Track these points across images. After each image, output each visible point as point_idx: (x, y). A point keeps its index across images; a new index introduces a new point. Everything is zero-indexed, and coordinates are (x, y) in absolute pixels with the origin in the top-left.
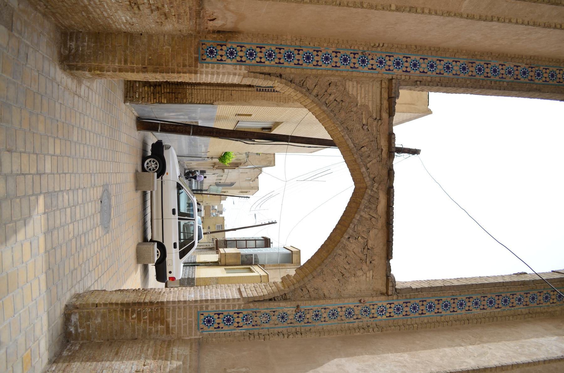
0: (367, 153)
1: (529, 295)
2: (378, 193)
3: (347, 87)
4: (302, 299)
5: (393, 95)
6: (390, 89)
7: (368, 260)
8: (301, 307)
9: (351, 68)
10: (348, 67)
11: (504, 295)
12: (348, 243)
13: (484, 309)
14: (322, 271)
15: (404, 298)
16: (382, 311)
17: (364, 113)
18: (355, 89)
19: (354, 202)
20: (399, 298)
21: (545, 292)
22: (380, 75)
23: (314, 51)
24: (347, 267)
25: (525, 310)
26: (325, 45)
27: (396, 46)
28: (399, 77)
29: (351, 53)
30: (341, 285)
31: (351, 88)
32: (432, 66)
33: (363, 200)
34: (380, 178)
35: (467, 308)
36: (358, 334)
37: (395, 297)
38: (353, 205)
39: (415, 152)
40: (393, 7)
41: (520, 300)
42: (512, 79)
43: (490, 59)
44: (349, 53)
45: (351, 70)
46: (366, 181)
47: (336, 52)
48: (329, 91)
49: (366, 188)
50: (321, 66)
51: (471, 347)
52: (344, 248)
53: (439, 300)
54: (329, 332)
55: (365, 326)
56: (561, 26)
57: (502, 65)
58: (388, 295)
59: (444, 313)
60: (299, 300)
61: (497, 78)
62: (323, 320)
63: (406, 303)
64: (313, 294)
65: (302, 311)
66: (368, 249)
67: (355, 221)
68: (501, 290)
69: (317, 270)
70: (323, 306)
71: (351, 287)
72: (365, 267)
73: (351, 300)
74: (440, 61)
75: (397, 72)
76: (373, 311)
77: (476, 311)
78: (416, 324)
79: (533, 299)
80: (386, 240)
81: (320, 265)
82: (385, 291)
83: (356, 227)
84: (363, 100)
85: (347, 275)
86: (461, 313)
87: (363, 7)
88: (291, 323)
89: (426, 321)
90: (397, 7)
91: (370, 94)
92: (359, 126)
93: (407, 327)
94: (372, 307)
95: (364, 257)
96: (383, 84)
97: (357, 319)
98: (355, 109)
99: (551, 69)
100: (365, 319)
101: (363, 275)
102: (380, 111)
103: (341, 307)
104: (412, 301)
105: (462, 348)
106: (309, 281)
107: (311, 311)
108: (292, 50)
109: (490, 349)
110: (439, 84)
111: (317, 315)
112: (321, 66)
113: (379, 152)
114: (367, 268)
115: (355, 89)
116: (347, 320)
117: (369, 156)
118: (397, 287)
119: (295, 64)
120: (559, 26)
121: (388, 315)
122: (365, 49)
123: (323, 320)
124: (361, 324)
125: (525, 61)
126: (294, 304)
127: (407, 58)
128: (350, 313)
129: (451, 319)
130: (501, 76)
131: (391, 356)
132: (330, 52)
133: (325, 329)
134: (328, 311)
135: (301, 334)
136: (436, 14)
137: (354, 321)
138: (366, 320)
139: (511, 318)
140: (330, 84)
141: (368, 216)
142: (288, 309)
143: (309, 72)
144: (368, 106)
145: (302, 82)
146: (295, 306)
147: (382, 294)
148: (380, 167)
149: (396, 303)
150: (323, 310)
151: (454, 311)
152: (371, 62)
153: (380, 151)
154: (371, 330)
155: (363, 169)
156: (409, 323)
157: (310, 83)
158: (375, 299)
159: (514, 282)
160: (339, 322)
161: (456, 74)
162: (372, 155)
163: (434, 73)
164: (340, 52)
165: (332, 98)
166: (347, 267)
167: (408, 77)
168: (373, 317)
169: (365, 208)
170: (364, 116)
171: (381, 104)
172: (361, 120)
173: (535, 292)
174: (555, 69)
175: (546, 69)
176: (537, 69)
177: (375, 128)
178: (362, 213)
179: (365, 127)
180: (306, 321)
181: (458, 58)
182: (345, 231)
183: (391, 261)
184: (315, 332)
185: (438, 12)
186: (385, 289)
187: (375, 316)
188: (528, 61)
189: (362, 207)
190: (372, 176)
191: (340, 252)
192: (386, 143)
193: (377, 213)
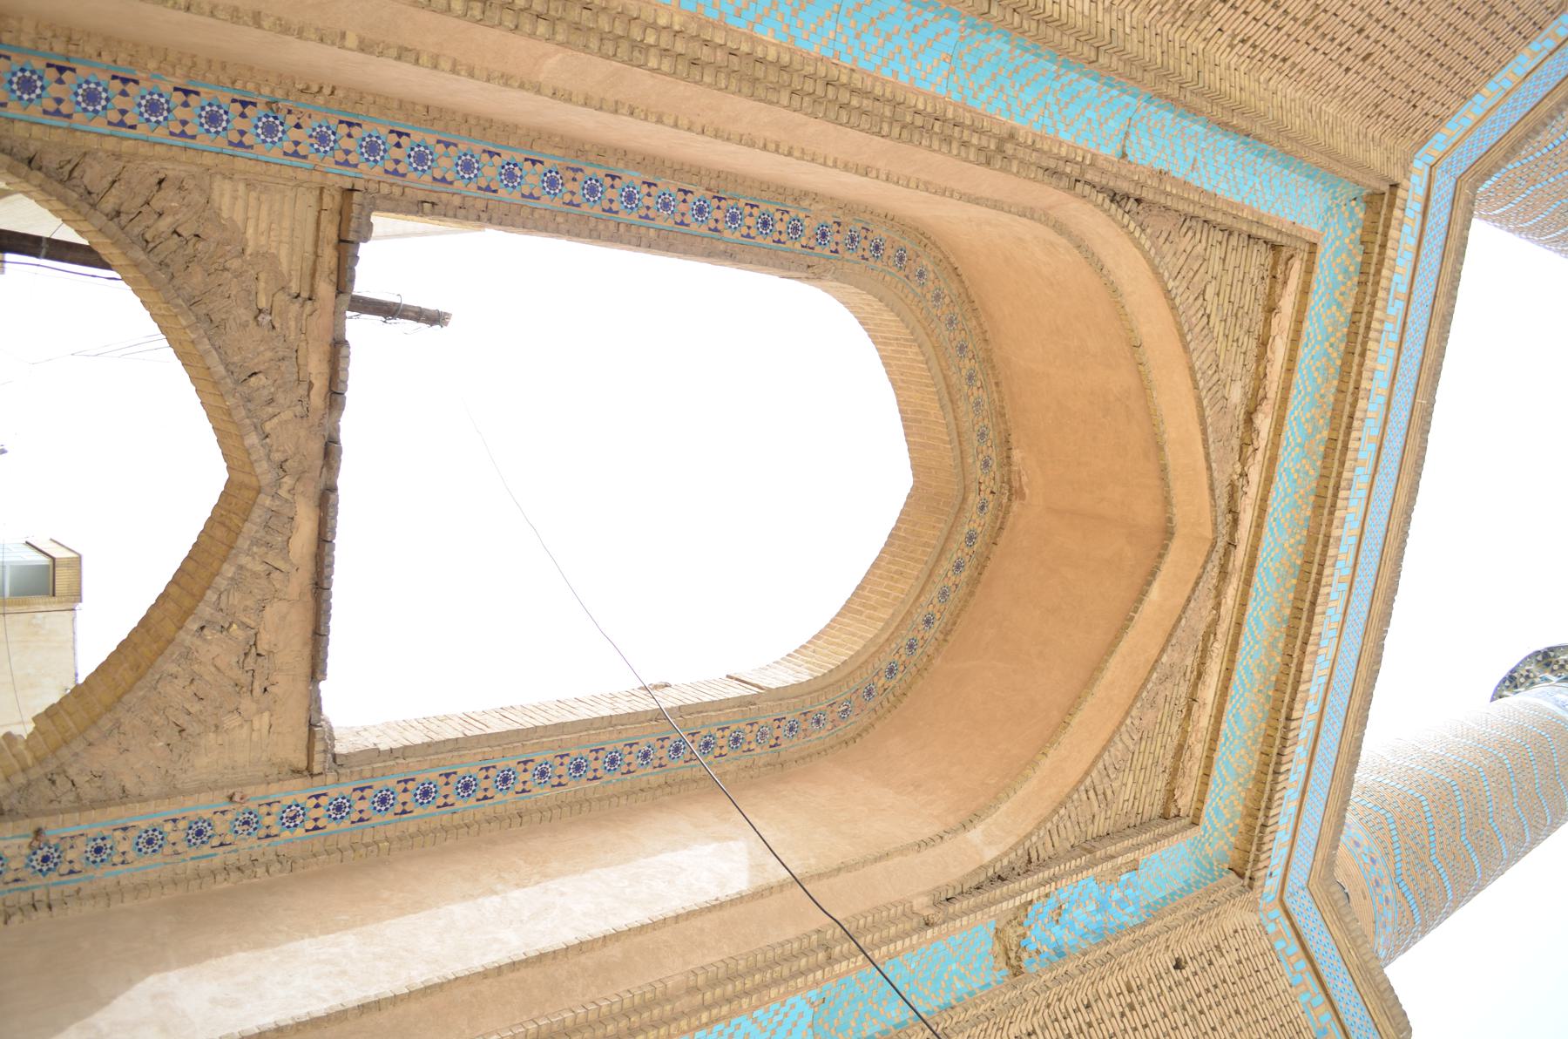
0: (266, 392)
1: (667, 743)
2: (293, 504)
3: (215, 195)
4: (51, 806)
5: (351, 237)
6: (343, 216)
7: (256, 684)
8: (48, 833)
9: (231, 143)
10: (221, 142)
11: (609, 748)
12: (198, 642)
13: (560, 785)
14: (118, 725)
15: (356, 777)
16: (293, 818)
17: (262, 276)
18: (240, 204)
19: (223, 524)
20: (343, 779)
21: (704, 733)
22: (317, 177)
23: (114, 77)
24: (195, 708)
25: (656, 778)
26: (152, 65)
27: (370, 98)
28: (372, 186)
29: (234, 101)
30: (175, 758)
31: (229, 199)
32: (467, 167)
33: (247, 525)
34: (300, 462)
35: (519, 787)
36: (225, 885)
37: (331, 777)
38: (220, 533)
39: (435, 319)
40: (352, 40)
41: (646, 755)
42: (669, 224)
43: (621, 165)
45: (229, 150)
46: (258, 471)
47: (187, 92)
48: (157, 204)
49: (259, 491)
50: (133, 127)
51: (517, 893)
52: (187, 655)
53: (447, 775)
54: (137, 890)
55: (245, 861)
56: (778, 146)
57: (650, 185)
58: (312, 775)
59: (460, 805)
60: (44, 814)
61: (634, 217)
62: (117, 859)
63: (362, 789)
64: (89, 791)
65: (53, 842)
67: (221, 582)
68: (603, 737)
69: (101, 723)
70: (120, 823)
71: (206, 760)
72: (246, 704)
73: (203, 797)
74: (491, 154)
75: (369, 172)
76: (267, 821)
77: (542, 793)
78: (387, 839)
79: (677, 750)
80: (310, 629)
81: (109, 709)
82: (303, 765)
83: (224, 597)
84: (263, 240)
85: (194, 728)
86: (505, 800)
87: (259, 26)
88: (16, 880)
89: (412, 829)
90: (361, 41)
91: (286, 223)
92: (245, 315)
93: (363, 851)
94: (265, 809)
95: (245, 679)
96: (326, 199)
97: (222, 845)
98: (235, 264)
99: (763, 207)
100: (244, 845)
101: (241, 726)
102: (313, 276)
103: (174, 821)
104: (378, 784)
105: (496, 899)
106: (76, 754)
107: (79, 842)
108: (39, 64)
109: (562, 894)
110: (483, 215)
111: (98, 850)
112: (133, 127)
113: (302, 390)
114: (254, 707)
115: (240, 204)
116: (193, 852)
117: (272, 400)
118: (340, 748)
119: (45, 112)
120: (772, 146)
121: (310, 825)
122: (279, 94)
123: (117, 859)
124: (232, 858)
125: (705, 180)
126: (28, 826)
127: (400, 134)
128: (199, 833)
129: (478, 817)
130: (643, 212)
131: (308, 946)
132: (166, 88)
133: (123, 882)
134: (132, 834)
135: (50, 907)
136: (471, 75)
138: (248, 845)
139: (623, 801)
140: (161, 182)
141: (260, 568)
142: (7, 843)
143: (92, 142)
144: (275, 257)
145: (69, 167)
146: (30, 832)
147: (296, 772)
148: (303, 433)
149: (334, 792)
150: (119, 834)
151: (485, 798)
152: (295, 134)
153: (305, 386)
154: (260, 871)
155: (252, 439)
156: (367, 839)
157: (93, 175)
158: (275, 787)
159: (636, 714)
160: (168, 860)
161: (531, 196)
162: (281, 398)
163: (473, 186)
164: (197, 93)
165: (165, 224)
166: (195, 708)
167: (397, 191)
168: (268, 836)
169: (252, 544)
170: (262, 285)
171: (317, 256)
172: (251, 295)
174: (772, 210)
175: (752, 206)
176: (731, 202)
177: (292, 324)
178: (244, 560)
179: (265, 319)
180: (64, 868)
181: (541, 153)
182: (189, 612)
183: (322, 685)
184: (94, 897)
185: (477, 72)
186: (304, 758)
187: (274, 831)
188: (713, 183)
189: (243, 543)
190: (277, 457)
191: (173, 668)
192: (325, 368)
193: (286, 559)
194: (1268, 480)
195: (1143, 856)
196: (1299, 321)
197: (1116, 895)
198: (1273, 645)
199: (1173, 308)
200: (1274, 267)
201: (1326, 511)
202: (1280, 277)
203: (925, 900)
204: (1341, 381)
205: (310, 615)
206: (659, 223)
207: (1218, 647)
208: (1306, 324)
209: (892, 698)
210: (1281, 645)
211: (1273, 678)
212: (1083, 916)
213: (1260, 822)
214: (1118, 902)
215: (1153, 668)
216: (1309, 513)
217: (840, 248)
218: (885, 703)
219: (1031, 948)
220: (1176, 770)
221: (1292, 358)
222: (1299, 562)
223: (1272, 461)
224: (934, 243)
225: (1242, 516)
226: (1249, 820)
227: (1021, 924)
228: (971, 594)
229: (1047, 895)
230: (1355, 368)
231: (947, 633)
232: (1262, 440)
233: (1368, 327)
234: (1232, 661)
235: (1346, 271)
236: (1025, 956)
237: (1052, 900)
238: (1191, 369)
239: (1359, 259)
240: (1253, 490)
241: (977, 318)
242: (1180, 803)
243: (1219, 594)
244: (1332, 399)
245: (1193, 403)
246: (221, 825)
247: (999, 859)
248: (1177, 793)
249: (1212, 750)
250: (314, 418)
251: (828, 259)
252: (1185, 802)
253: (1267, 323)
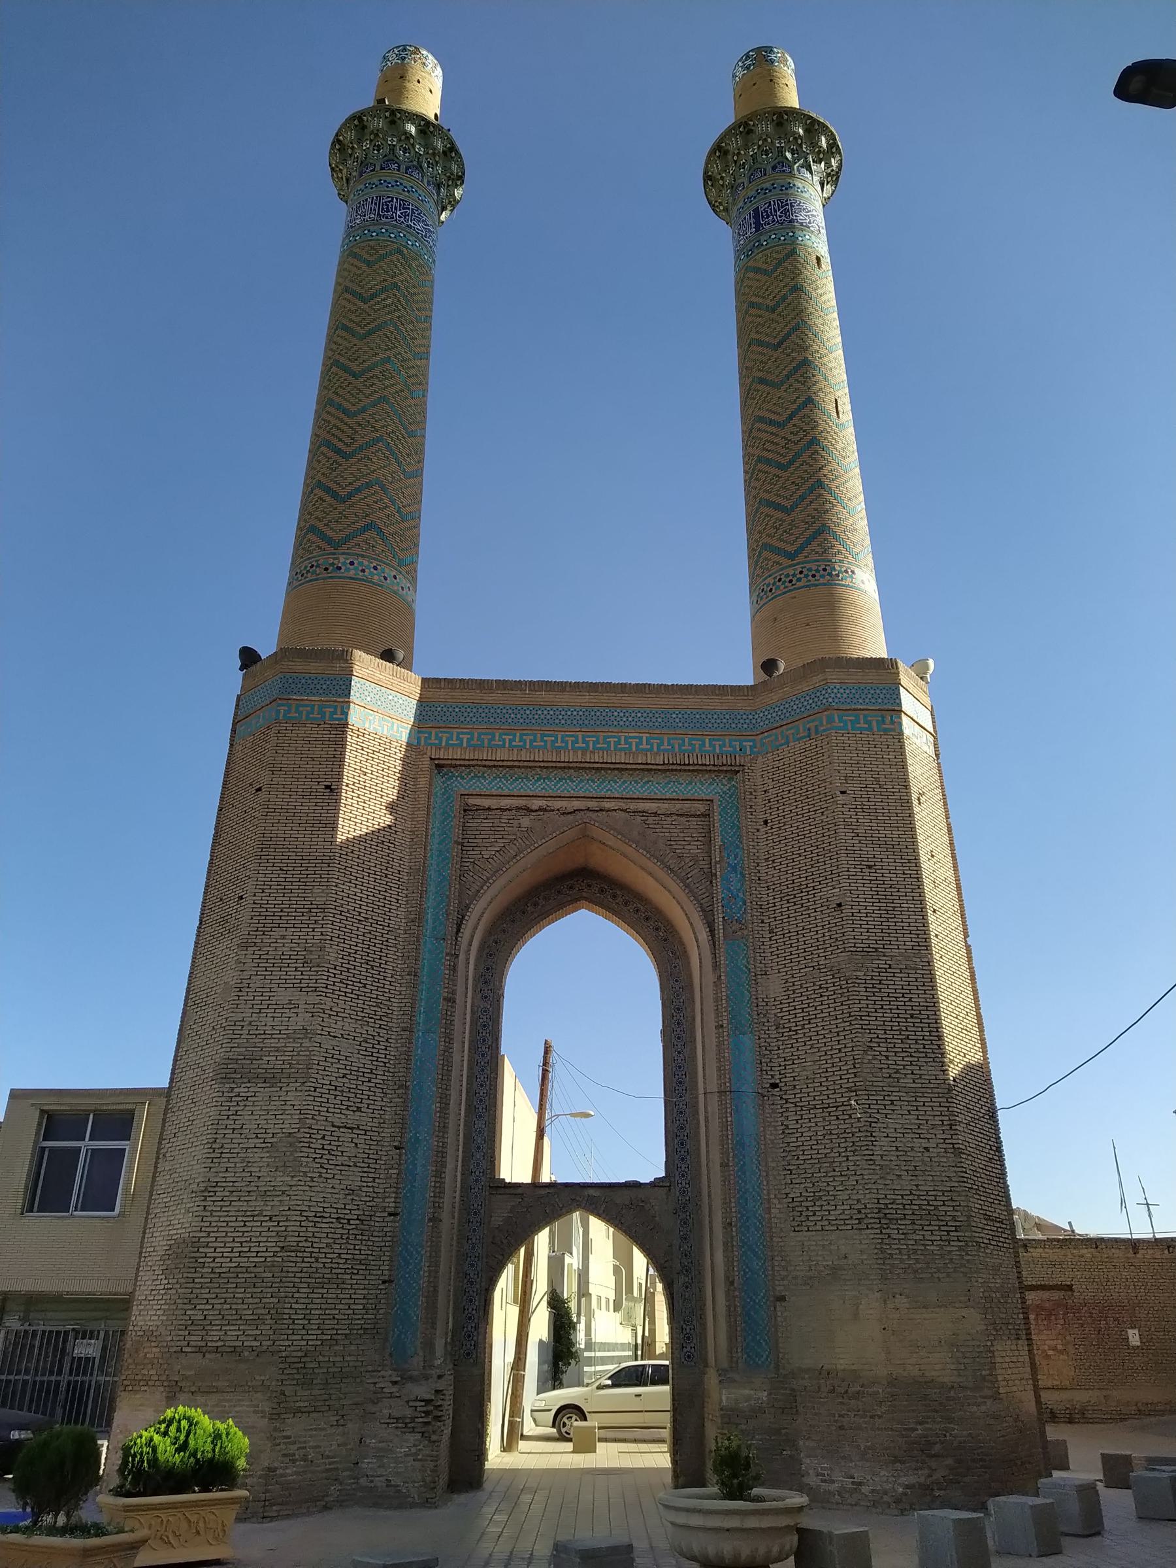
39: (547, 1050)
207: (632, 806)
235: (469, 773)
242: (703, 810)
246: (683, 1216)
252: (701, 808)
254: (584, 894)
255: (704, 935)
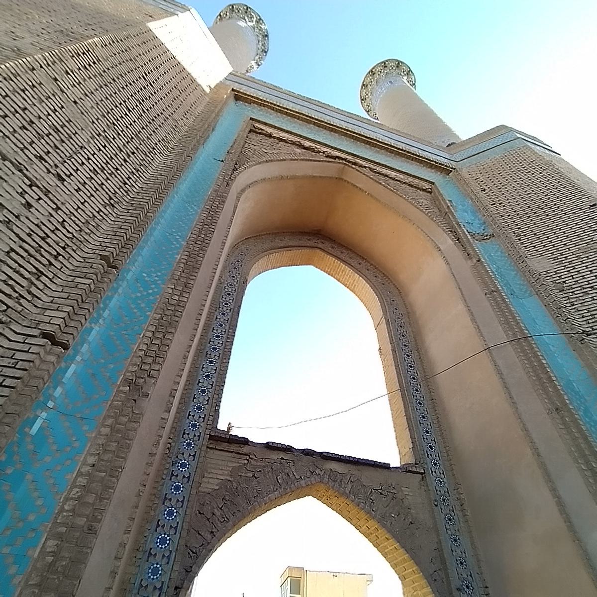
3: (206, 490)
9: (188, 482)
44: (170, 482)
45: (190, 483)
66: (381, 489)
80: (372, 468)
91: (220, 463)
96: (211, 446)
101: (407, 499)
115: (211, 480)
117: (287, 474)
137: (456, 515)
140: (200, 513)
141: (350, 486)
143: (182, 542)
146: (458, 593)
153: (282, 460)
167: (211, 418)
173: (401, 343)
181: (200, 365)
190: (309, 474)
192: (276, 452)
194: (326, 145)
195: (447, 198)
196: (275, 127)
197: (460, 207)
198: (378, 152)
199: (272, 161)
200: (256, 132)
201: (337, 129)
202: (260, 131)
203: (469, 262)
204: (295, 118)
205: (366, 468)
206: (227, 328)
207: (378, 169)
208: (276, 125)
209: (385, 278)
210: (378, 150)
211: (389, 153)
212: (468, 217)
213: (434, 163)
214: (463, 206)
215: (386, 187)
216: (337, 135)
217: (238, 272)
218: (387, 280)
219: (483, 232)
220: (416, 187)
221: (287, 132)
222: (352, 140)
223: (320, 143)
224: (238, 244)
225: (337, 155)
226: (433, 167)
227: (474, 234)
228: (351, 250)
229: (464, 226)
230: (292, 112)
231: (364, 259)
232: (314, 145)
233: (278, 106)
234: (383, 165)
235: (259, 111)
236: (486, 234)
237: (464, 224)
238: (291, 160)
239: (256, 105)
240: (329, 150)
241: (262, 235)
243: (361, 166)
244: (301, 122)
245: (301, 162)
247: (452, 240)
248: (424, 188)
249: (410, 175)
250: (295, 459)
251: (241, 277)
253: (275, 138)
254: (320, 245)
255: (447, 242)
